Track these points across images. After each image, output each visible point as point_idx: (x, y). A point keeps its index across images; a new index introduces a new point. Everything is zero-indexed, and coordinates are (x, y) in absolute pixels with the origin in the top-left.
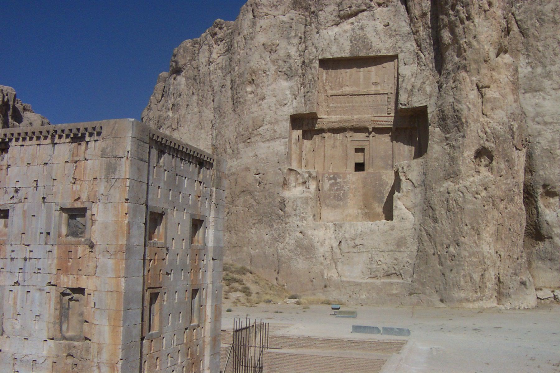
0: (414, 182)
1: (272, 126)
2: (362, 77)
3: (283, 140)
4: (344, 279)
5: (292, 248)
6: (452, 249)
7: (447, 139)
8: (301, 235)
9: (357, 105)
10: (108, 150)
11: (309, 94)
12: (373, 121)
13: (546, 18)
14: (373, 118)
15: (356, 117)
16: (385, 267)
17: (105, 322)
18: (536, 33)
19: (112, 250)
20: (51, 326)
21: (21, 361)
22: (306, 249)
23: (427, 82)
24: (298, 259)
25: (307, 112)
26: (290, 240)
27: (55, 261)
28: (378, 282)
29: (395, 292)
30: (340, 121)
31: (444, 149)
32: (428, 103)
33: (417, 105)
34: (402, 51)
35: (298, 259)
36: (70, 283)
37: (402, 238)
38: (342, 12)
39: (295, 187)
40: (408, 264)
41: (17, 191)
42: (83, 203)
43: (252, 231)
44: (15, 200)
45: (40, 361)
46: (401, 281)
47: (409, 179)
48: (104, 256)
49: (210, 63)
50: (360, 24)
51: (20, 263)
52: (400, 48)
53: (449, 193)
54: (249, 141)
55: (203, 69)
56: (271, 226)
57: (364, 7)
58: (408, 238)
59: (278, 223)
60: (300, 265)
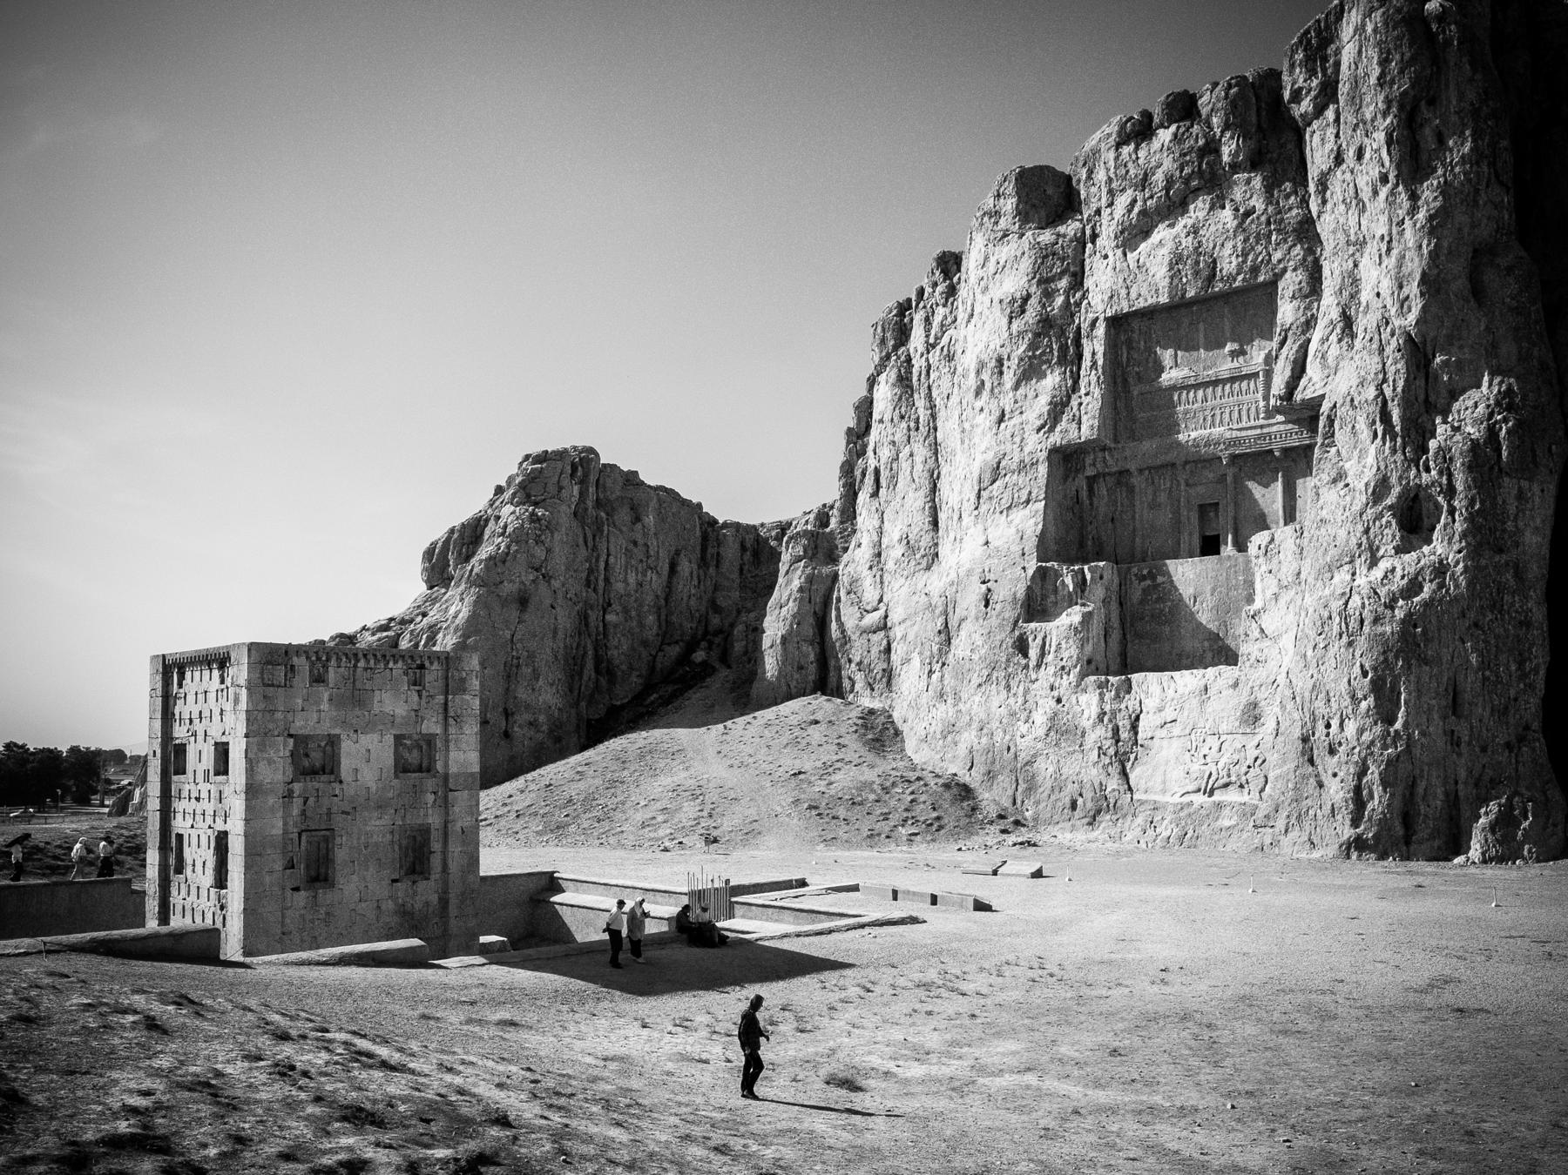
14: (1228, 435)
15: (1194, 435)
28: (1199, 799)
29: (1227, 823)
43: (977, 699)
49: (930, 347)
50: (1190, 222)
55: (918, 363)
56: (1008, 687)
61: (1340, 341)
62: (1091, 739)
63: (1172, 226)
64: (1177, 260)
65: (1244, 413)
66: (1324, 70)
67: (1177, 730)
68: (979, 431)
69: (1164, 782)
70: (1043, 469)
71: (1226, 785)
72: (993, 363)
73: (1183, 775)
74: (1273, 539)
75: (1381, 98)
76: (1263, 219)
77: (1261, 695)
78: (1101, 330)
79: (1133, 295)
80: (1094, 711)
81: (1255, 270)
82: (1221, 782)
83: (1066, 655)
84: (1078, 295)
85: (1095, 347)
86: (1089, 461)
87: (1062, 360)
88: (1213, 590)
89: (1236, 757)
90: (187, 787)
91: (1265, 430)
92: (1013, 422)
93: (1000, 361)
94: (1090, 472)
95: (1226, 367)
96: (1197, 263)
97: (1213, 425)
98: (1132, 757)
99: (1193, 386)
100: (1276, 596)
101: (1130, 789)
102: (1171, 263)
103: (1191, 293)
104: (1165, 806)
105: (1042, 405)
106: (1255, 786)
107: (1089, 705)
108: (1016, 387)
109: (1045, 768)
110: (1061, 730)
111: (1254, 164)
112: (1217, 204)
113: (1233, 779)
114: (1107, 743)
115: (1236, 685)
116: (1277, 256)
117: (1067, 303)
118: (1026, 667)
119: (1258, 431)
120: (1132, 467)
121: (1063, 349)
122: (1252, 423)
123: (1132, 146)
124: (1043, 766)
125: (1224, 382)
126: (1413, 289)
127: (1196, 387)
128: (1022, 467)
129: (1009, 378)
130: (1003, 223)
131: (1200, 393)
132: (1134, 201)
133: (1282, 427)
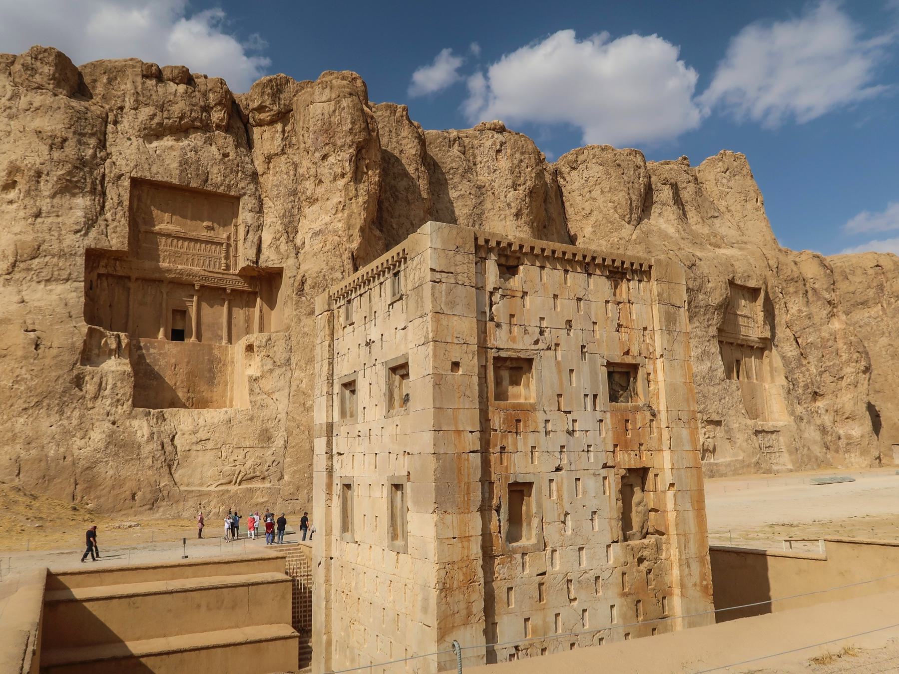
1: (55, 260)
3: (76, 284)
4: (182, 488)
5: (102, 445)
10: (665, 295)
11: (115, 223)
12: (206, 278)
13: (400, 196)
14: (203, 273)
15: (180, 267)
16: (242, 469)
17: (688, 506)
18: (390, 209)
19: (685, 417)
20: (614, 523)
21: (579, 582)
25: (114, 249)
27: (610, 434)
28: (233, 488)
29: (261, 500)
32: (284, 265)
36: (632, 462)
38: (166, 121)
39: (98, 355)
40: (275, 464)
41: (542, 333)
42: (634, 357)
44: (541, 345)
45: (605, 575)
46: (267, 485)
48: (677, 425)
50: (192, 144)
51: (563, 439)
54: (8, 277)
56: (61, 412)
57: (198, 124)
58: (271, 430)
59: (75, 408)
61: (287, 242)
62: (146, 450)
63: (177, 140)
64: (184, 163)
65: (212, 263)
66: (279, 104)
67: (210, 445)
68: (7, 217)
69: (202, 478)
70: (80, 261)
71: (253, 478)
72: (32, 173)
73: (217, 473)
74: (270, 339)
75: (351, 138)
76: (235, 162)
77: (270, 425)
78: (127, 183)
79: (154, 169)
80: (146, 431)
81: (229, 187)
82: (249, 476)
83: (122, 391)
84: (103, 154)
85: (118, 194)
86: (103, 263)
87: (93, 191)
88: (188, 362)
89: (259, 461)
90: (540, 417)
91: (225, 276)
92: (50, 220)
93: (39, 174)
94: (102, 271)
95: (205, 234)
96: (198, 169)
97: (192, 264)
98: (176, 462)
99: (182, 238)
100: (271, 371)
101: (176, 484)
102: (180, 163)
103: (193, 185)
104: (209, 494)
105: (78, 215)
106: (274, 478)
107: (141, 428)
108: (53, 196)
109: (107, 471)
110: (119, 445)
111: (228, 129)
112: (209, 141)
113: (258, 474)
114: (158, 454)
115: (251, 419)
116: (241, 185)
117: (94, 156)
118: (83, 397)
119: (221, 276)
120: (134, 275)
121: (93, 183)
122: (217, 270)
123: (154, 82)
124: (103, 470)
125: (202, 242)
126: (356, 232)
127: (185, 239)
128: (62, 254)
129: (46, 188)
130: (38, 78)
131: (186, 243)
132: (155, 115)
133: (234, 277)
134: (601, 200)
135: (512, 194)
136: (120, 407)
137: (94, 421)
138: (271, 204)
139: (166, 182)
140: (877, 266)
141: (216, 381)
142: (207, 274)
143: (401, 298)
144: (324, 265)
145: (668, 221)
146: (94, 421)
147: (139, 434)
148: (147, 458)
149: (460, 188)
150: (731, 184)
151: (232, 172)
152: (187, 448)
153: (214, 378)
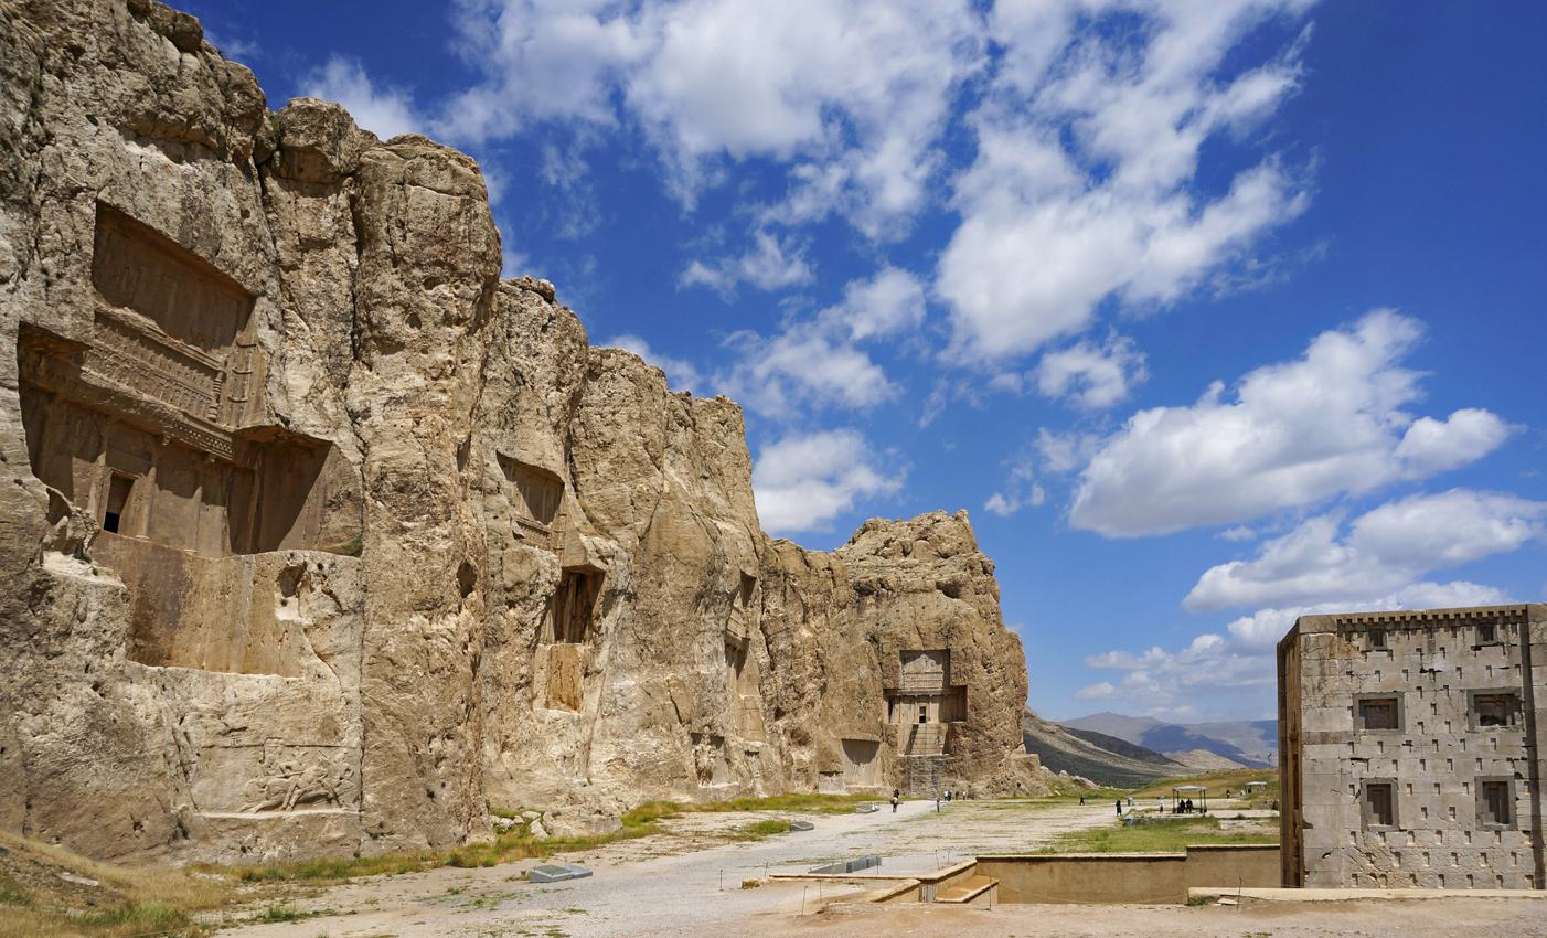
0: (342, 601)
2: (171, 302)
5: (78, 729)
6: (436, 744)
7: (404, 530)
8: (96, 695)
9: (152, 367)
11: (65, 284)
15: (146, 397)
22: (112, 734)
23: (325, 392)
24: (96, 765)
26: (70, 707)
30: (107, 393)
31: (404, 549)
32: (334, 439)
33: (310, 431)
34: (264, 294)
35: (96, 765)
37: (328, 717)
40: (348, 775)
47: (330, 593)
52: (263, 283)
53: (427, 638)
58: (338, 718)
60: (96, 778)
67: (245, 739)
91: (212, 433)
119: (207, 430)
134: (626, 430)
135: (554, 394)
136: (107, 656)
137: (61, 680)
138: (303, 324)
139: (159, 233)
140: (829, 569)
141: (180, 621)
142: (186, 421)
143: (1496, 645)
144: (420, 457)
145: (679, 474)
146: (61, 680)
147: (140, 711)
148: (155, 757)
149: (494, 367)
150: (727, 440)
151: (251, 249)
152: (209, 743)
153: (179, 615)
